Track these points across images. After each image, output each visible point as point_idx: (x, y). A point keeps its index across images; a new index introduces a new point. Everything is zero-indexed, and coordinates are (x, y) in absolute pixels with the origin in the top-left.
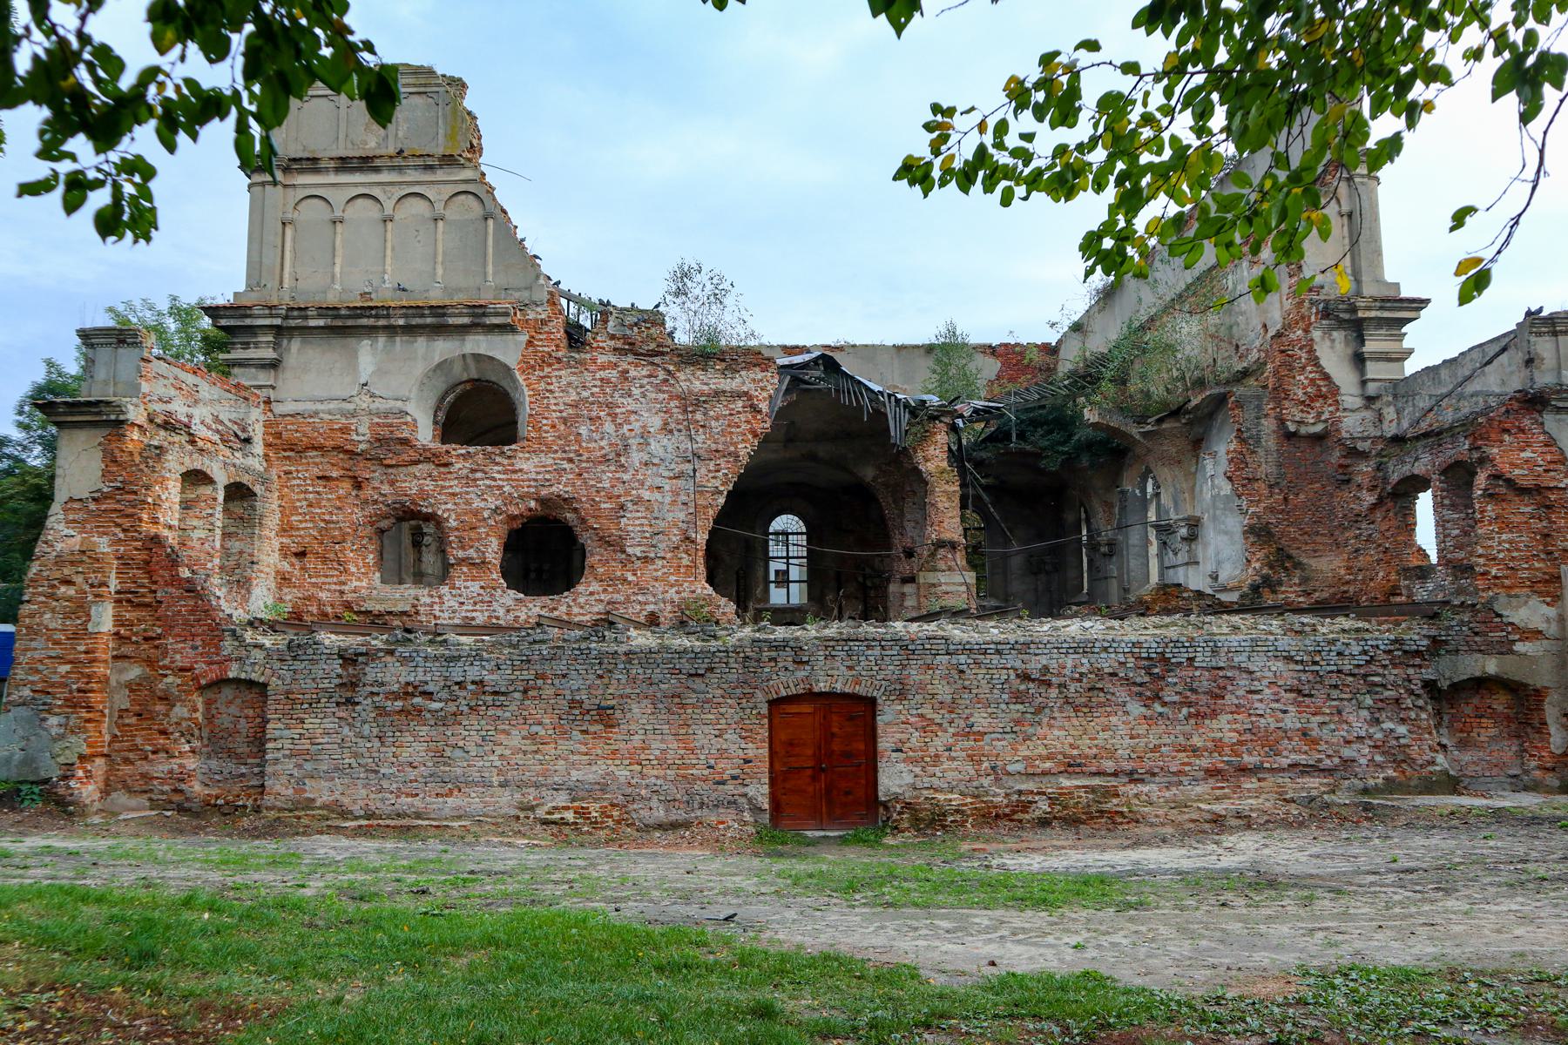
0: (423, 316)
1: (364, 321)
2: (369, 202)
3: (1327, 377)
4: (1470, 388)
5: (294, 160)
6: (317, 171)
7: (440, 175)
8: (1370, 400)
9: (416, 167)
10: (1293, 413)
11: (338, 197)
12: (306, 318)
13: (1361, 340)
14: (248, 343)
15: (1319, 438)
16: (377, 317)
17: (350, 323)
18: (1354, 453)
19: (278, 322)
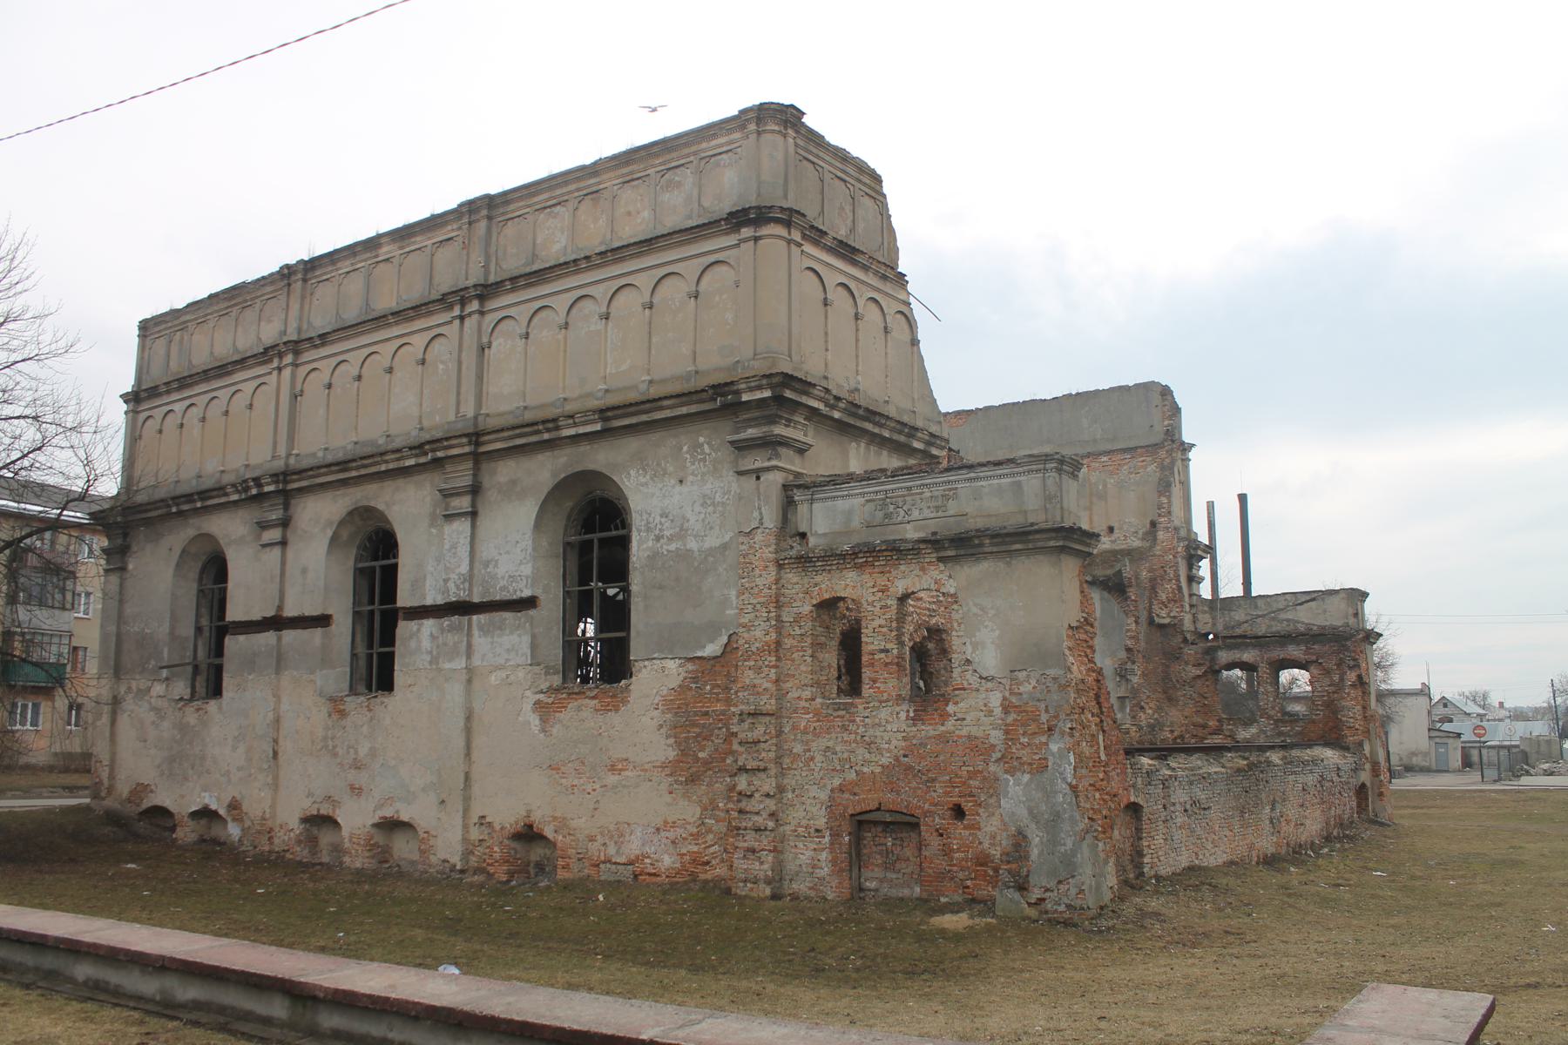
0: (900, 432)
1: (869, 426)
2: (845, 293)
3: (1180, 588)
4: (1283, 616)
5: (812, 227)
6: (816, 243)
7: (888, 288)
8: (1191, 606)
9: (876, 273)
10: (1155, 607)
11: (832, 279)
12: (833, 407)
13: (1190, 567)
14: (789, 421)
15: (1162, 626)
16: (876, 424)
17: (859, 423)
18: (1185, 640)
19: (821, 406)
